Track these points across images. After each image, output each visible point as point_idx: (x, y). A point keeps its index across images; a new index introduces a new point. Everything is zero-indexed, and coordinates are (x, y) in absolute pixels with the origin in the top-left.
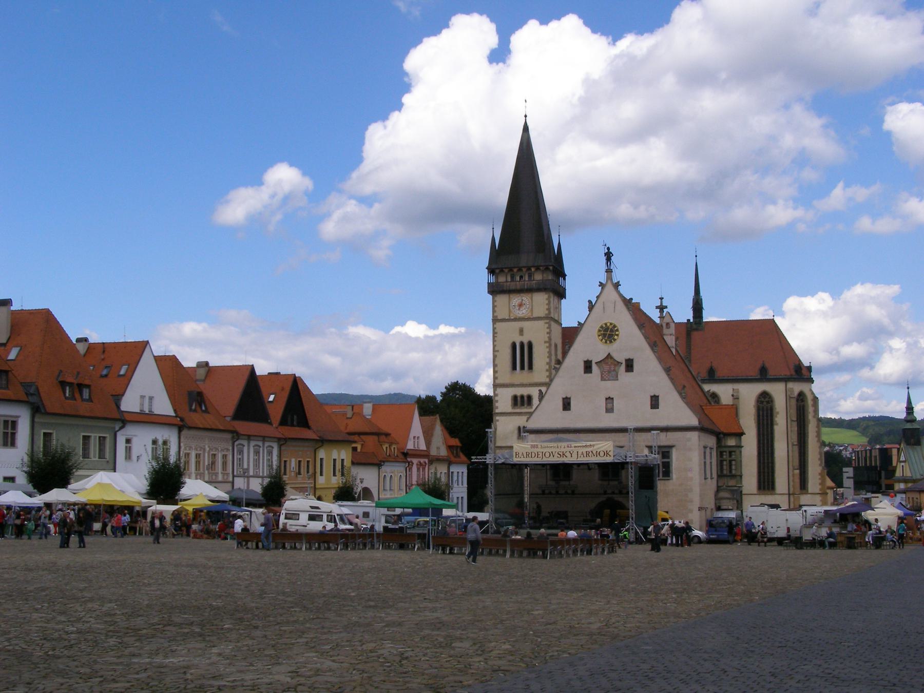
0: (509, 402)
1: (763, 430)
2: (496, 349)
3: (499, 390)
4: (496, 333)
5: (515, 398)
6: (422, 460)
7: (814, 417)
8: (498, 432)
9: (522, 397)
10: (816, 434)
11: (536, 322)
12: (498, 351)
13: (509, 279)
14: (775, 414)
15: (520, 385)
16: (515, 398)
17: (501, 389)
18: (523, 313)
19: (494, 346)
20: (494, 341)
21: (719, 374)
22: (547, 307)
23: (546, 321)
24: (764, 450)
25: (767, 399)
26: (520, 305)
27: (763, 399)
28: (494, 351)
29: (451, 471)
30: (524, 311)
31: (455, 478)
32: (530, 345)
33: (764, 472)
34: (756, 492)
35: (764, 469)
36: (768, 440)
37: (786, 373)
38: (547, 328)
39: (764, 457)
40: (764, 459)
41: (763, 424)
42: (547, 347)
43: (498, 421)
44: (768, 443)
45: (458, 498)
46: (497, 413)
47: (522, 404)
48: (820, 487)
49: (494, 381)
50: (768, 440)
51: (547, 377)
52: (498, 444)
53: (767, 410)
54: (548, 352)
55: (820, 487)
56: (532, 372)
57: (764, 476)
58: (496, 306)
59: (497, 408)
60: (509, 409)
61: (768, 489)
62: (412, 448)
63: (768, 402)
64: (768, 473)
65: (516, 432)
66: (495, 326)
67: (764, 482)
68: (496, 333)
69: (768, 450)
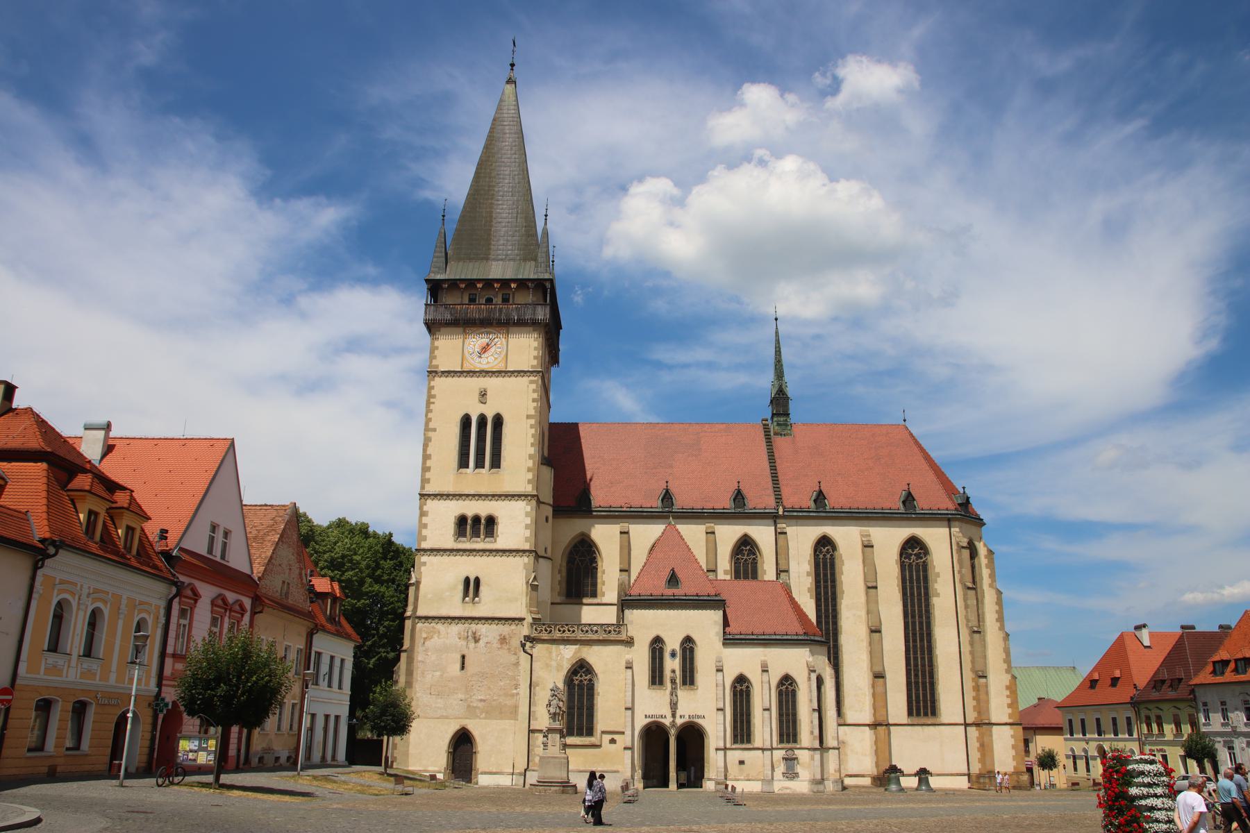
0: (451, 527)
1: (913, 605)
2: (431, 425)
3: (431, 505)
4: (434, 396)
5: (462, 521)
6: (231, 597)
7: (991, 586)
8: (422, 586)
9: (477, 519)
10: (996, 616)
11: (513, 379)
12: (434, 430)
13: (466, 300)
14: (931, 576)
15: (474, 496)
16: (462, 521)
17: (436, 502)
18: (488, 363)
19: (428, 421)
20: (428, 411)
21: (833, 501)
22: (535, 353)
23: (532, 378)
24: (915, 641)
25: (916, 551)
26: (485, 349)
27: (910, 551)
28: (427, 429)
29: (314, 649)
30: (491, 359)
31: (324, 668)
32: (498, 421)
33: (917, 683)
34: (904, 719)
35: (916, 675)
36: (921, 623)
37: (947, 505)
38: (534, 391)
39: (915, 653)
40: (916, 659)
41: (912, 594)
42: (532, 426)
43: (424, 564)
44: (921, 629)
45: (327, 717)
46: (425, 550)
47: (476, 534)
48: (1010, 711)
49: (423, 487)
50: (921, 623)
51: (529, 482)
52: (420, 613)
53: (918, 571)
54: (533, 436)
55: (1010, 711)
56: (498, 471)
57: (917, 690)
58: (437, 348)
59: (425, 539)
60: (450, 543)
61: (926, 714)
62: (203, 551)
63: (918, 556)
64: (924, 683)
65: (461, 587)
66: (432, 383)
67: (918, 702)
68: (434, 396)
69: (922, 640)
